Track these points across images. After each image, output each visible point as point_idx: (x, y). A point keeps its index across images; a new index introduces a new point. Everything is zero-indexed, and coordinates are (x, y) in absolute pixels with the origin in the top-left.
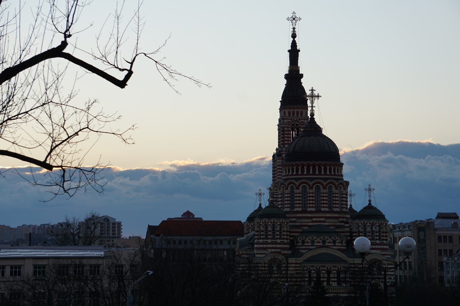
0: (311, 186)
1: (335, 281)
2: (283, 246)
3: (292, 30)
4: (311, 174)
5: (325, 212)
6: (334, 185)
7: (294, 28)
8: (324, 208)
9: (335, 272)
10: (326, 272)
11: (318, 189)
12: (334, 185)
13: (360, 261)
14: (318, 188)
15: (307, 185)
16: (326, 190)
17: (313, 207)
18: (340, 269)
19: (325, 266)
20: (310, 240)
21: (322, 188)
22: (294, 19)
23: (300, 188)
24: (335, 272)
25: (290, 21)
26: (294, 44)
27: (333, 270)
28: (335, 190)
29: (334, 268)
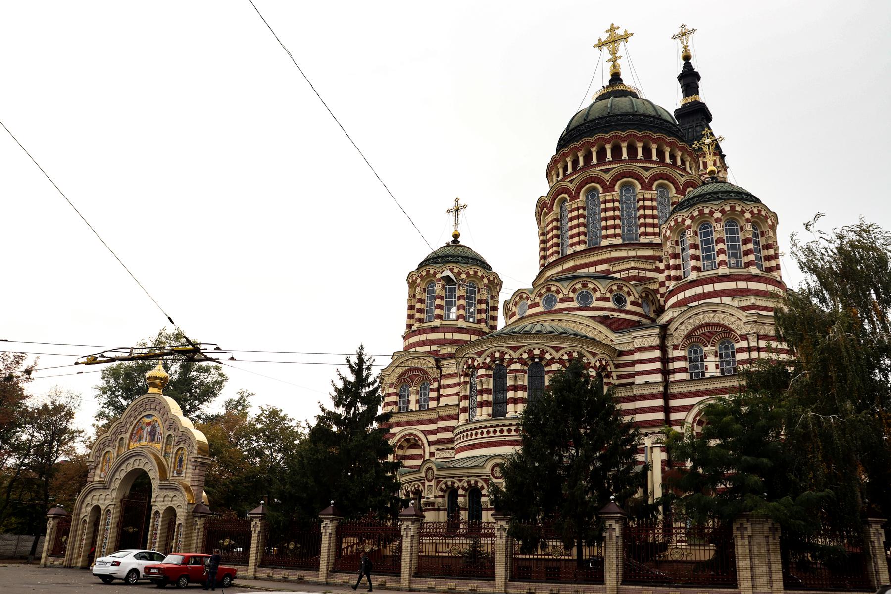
0: (573, 192)
1: (515, 401)
2: (448, 336)
3: (683, 49)
4: (580, 169)
5: (611, 246)
6: (638, 178)
7: (685, 48)
8: (608, 239)
9: (517, 366)
10: (491, 372)
11: (593, 196)
12: (637, 179)
13: (652, 338)
14: (592, 192)
15: (566, 193)
16: (613, 193)
17: (579, 243)
18: (541, 357)
19: (483, 352)
20: (518, 306)
21: (601, 190)
22: (684, 34)
23: (554, 207)
24: (517, 366)
25: (678, 39)
26: (688, 67)
27: (511, 361)
28: (642, 189)
29: (512, 353)
